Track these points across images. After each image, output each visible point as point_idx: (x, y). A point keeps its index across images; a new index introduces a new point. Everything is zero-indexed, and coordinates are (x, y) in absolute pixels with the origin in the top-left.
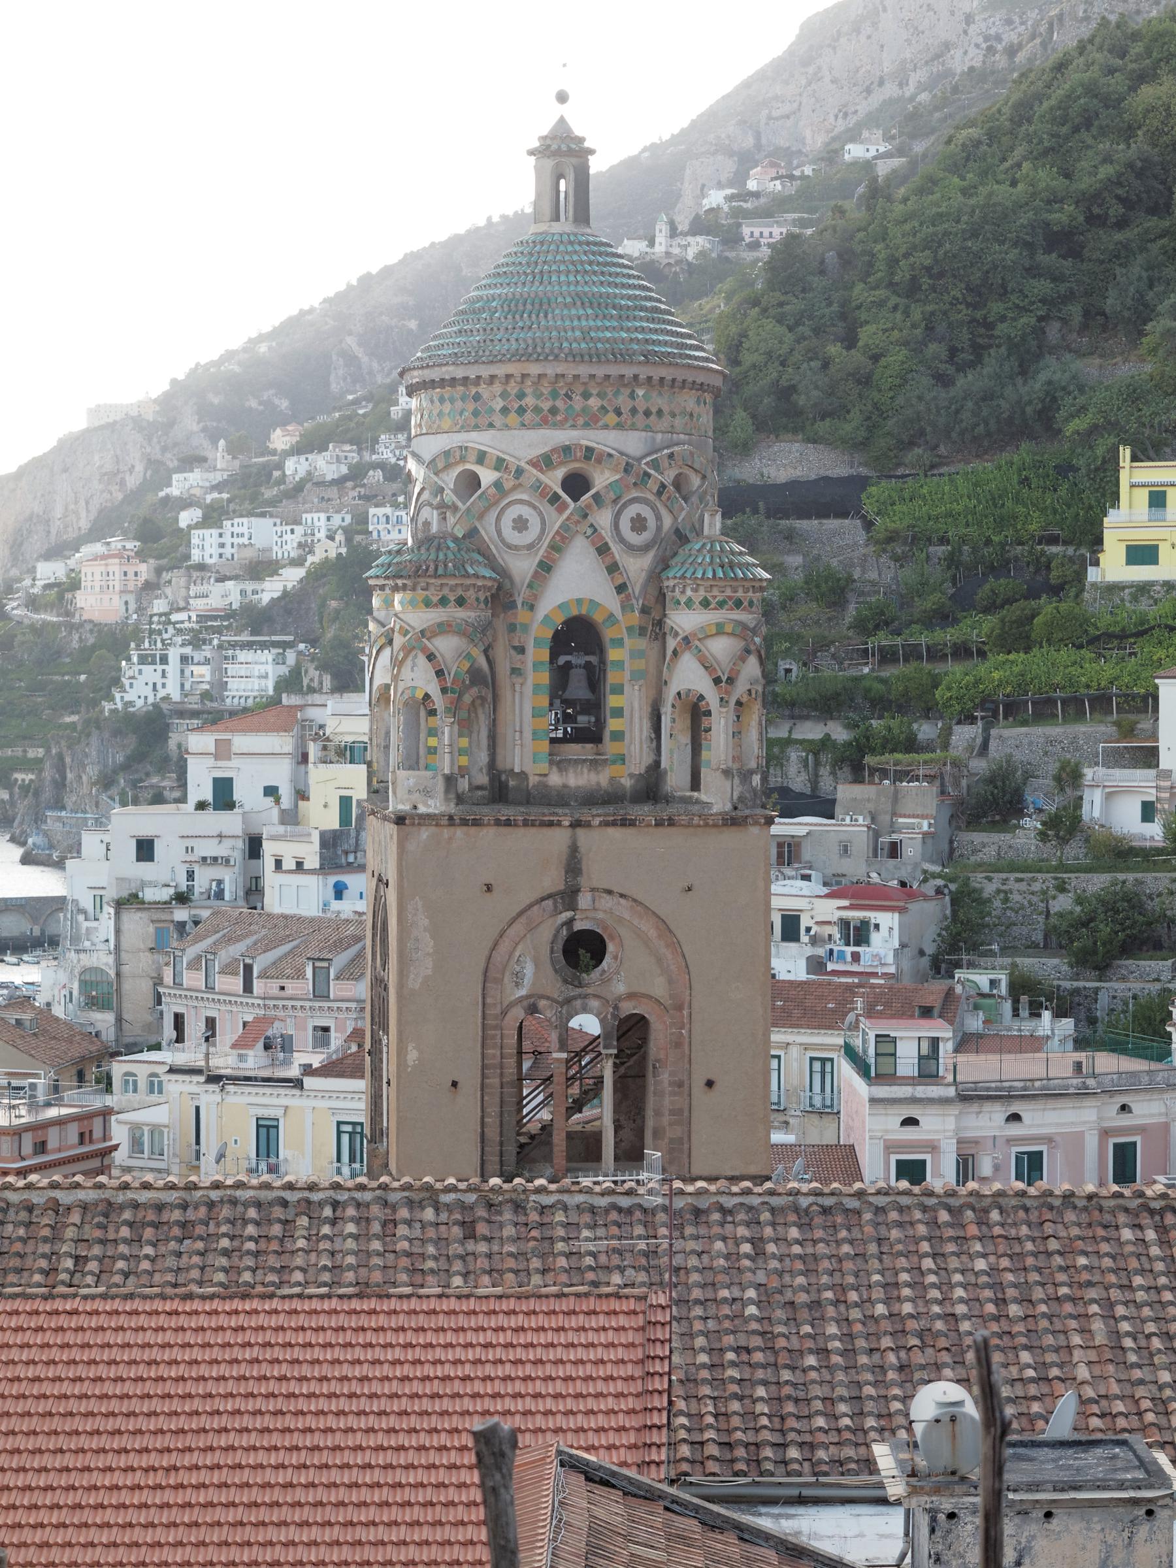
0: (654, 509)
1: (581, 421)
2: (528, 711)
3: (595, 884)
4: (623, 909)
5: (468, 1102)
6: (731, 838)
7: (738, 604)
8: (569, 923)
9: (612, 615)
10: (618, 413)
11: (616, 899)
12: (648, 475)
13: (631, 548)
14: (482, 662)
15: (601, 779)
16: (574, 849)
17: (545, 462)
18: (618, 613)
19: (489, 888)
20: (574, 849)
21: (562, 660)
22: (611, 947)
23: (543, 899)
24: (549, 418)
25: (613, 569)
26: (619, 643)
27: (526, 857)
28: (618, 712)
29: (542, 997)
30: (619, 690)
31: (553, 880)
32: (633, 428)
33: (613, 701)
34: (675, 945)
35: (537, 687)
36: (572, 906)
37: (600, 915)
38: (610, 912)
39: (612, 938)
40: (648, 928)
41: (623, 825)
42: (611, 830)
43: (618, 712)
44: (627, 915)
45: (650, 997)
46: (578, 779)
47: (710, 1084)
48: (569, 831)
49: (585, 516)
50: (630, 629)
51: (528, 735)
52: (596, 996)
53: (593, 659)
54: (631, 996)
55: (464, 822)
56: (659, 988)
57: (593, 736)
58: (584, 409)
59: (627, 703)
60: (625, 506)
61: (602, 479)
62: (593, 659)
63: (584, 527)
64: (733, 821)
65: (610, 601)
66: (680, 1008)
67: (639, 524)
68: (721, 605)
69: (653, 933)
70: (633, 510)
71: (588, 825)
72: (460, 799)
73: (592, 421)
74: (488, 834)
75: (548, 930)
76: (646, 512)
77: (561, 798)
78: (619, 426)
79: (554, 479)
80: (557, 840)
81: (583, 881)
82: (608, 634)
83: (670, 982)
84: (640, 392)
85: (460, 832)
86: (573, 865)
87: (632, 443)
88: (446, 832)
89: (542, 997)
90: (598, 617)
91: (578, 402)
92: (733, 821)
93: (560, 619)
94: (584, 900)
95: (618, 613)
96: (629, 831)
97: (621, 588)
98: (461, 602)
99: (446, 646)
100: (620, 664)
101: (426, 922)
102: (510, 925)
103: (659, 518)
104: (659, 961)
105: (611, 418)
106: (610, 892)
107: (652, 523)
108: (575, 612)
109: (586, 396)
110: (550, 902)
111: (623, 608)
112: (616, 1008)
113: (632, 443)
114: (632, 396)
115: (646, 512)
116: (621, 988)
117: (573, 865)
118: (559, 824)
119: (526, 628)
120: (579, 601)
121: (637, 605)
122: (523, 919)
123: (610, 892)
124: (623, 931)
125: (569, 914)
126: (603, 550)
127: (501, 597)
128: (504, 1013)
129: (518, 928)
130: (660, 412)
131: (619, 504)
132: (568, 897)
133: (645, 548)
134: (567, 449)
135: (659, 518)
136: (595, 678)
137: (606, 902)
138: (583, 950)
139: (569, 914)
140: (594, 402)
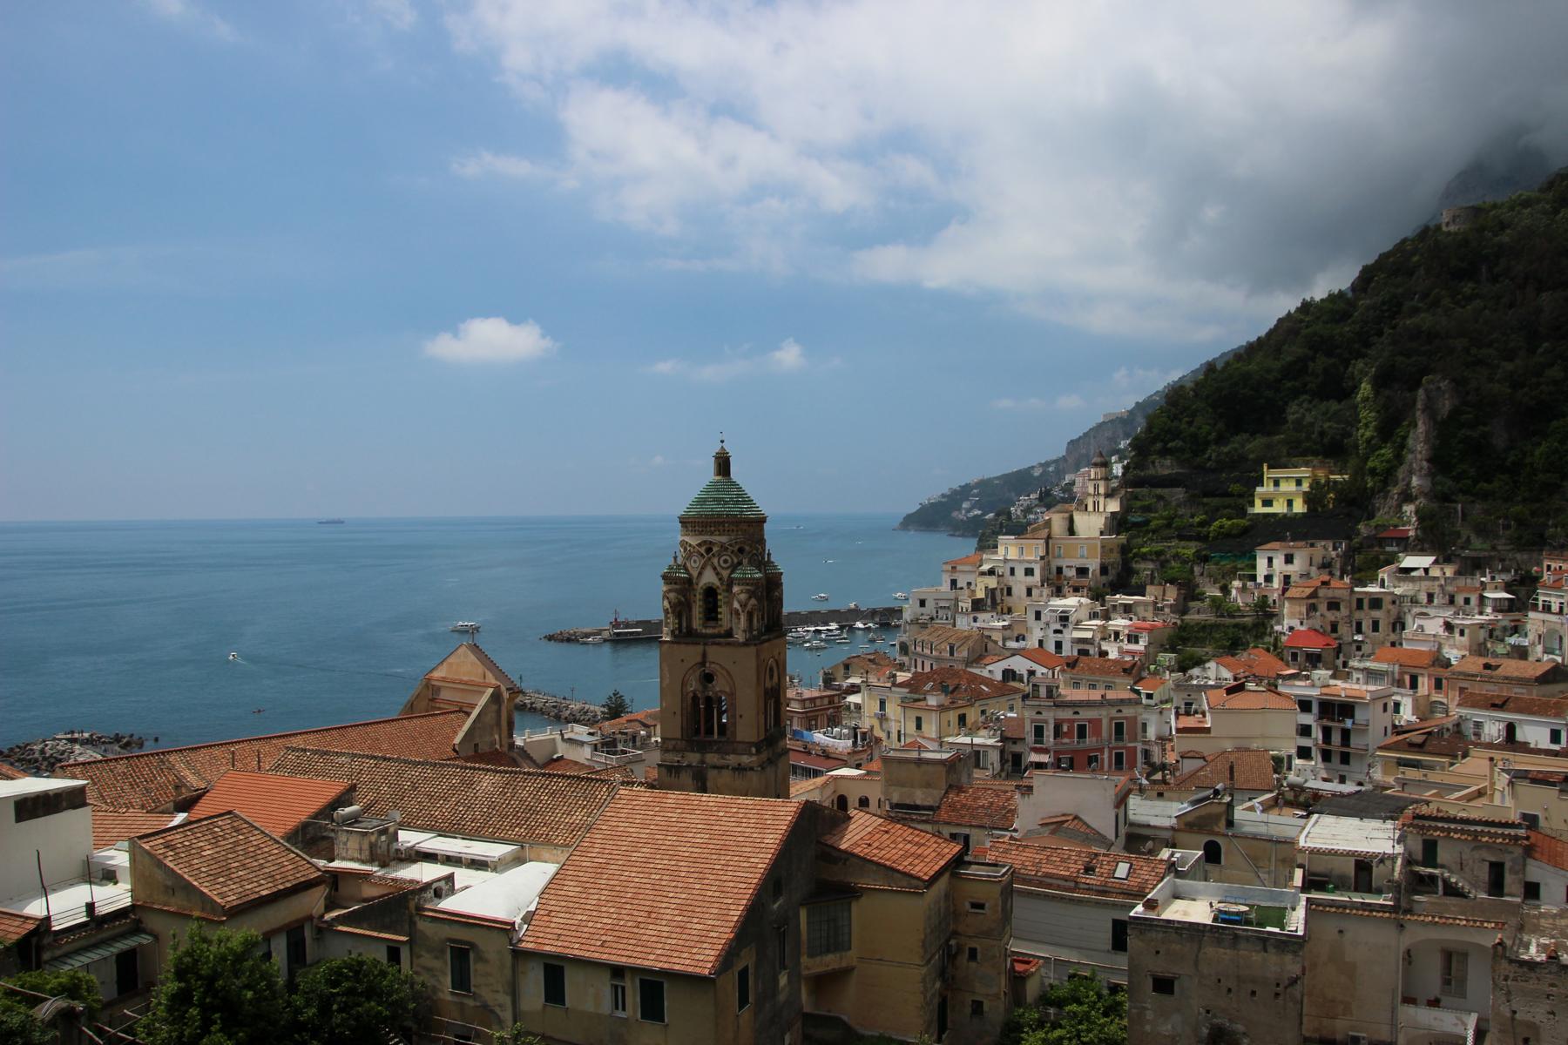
5: (679, 717)
15: (716, 631)
24: (701, 533)
27: (692, 653)
31: (699, 659)
46: (709, 631)
57: (716, 619)
59: (723, 610)
61: (715, 549)
64: (746, 644)
65: (717, 583)
73: (712, 534)
74: (683, 647)
77: (705, 636)
79: (702, 550)
80: (700, 648)
86: (704, 655)
87: (724, 539)
92: (746, 644)
99: (672, 595)
113: (724, 539)
117: (704, 655)
127: (689, 581)
132: (703, 664)
138: (708, 678)
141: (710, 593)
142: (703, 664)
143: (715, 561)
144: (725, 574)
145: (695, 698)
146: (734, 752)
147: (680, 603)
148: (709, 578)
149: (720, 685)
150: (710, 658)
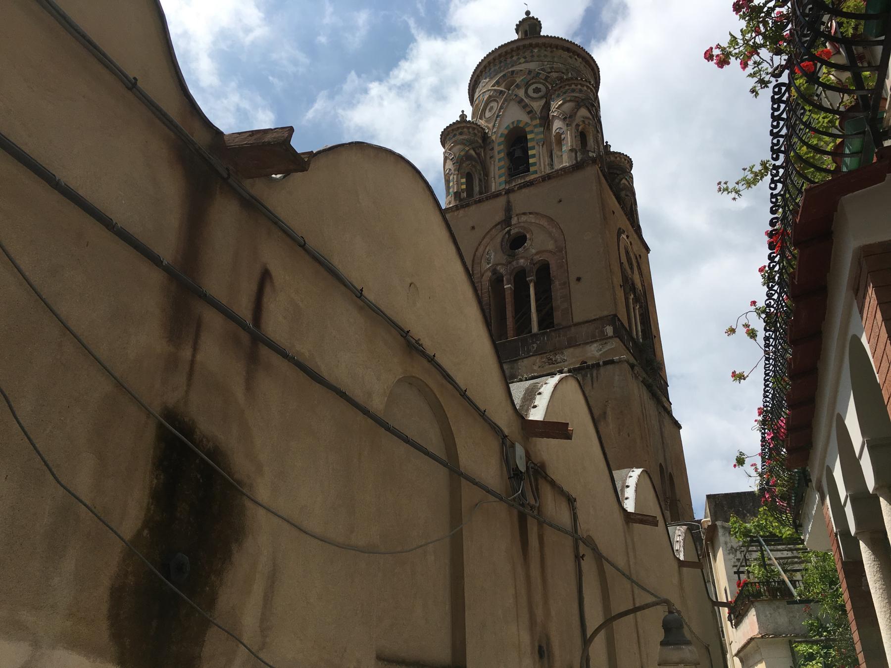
0: (544, 84)
2: (497, 168)
3: (518, 212)
4: (532, 219)
7: (573, 91)
8: (509, 232)
10: (525, 58)
13: (533, 99)
14: (472, 152)
16: (508, 202)
17: (498, 83)
18: (529, 121)
19: (473, 228)
20: (508, 202)
22: (528, 236)
23: (496, 225)
25: (525, 106)
26: (532, 132)
28: (534, 156)
29: (497, 265)
30: (533, 148)
31: (500, 216)
33: (530, 152)
36: (509, 225)
37: (522, 224)
40: (544, 222)
42: (523, 190)
43: (534, 156)
47: (579, 279)
50: (535, 126)
52: (522, 258)
54: (537, 254)
55: (463, 207)
56: (551, 246)
60: (530, 85)
65: (524, 118)
67: (537, 90)
68: (565, 93)
70: (534, 86)
72: (461, 200)
76: (539, 86)
78: (526, 62)
82: (527, 129)
83: (556, 241)
85: (461, 212)
86: (508, 209)
87: (532, 66)
88: (456, 214)
89: (497, 265)
90: (521, 125)
91: (509, 61)
93: (506, 132)
94: (514, 221)
95: (529, 121)
97: (529, 113)
98: (461, 134)
100: (532, 139)
102: (484, 238)
103: (547, 88)
105: (522, 60)
106: (524, 214)
107: (543, 89)
109: (512, 57)
111: (532, 119)
113: (532, 66)
114: (532, 52)
115: (539, 86)
116: (534, 251)
117: (508, 209)
120: (513, 123)
122: (488, 236)
123: (524, 214)
128: (482, 275)
130: (545, 56)
131: (527, 85)
132: (507, 221)
133: (541, 98)
135: (547, 88)
136: (525, 150)
137: (523, 218)
138: (517, 242)
140: (515, 58)
141: (517, 140)
142: (507, 221)
143: (521, 93)
144: (537, 106)
145: (497, 280)
146: (573, 343)
147: (468, 157)
148: (515, 115)
149: (538, 245)
150: (517, 208)
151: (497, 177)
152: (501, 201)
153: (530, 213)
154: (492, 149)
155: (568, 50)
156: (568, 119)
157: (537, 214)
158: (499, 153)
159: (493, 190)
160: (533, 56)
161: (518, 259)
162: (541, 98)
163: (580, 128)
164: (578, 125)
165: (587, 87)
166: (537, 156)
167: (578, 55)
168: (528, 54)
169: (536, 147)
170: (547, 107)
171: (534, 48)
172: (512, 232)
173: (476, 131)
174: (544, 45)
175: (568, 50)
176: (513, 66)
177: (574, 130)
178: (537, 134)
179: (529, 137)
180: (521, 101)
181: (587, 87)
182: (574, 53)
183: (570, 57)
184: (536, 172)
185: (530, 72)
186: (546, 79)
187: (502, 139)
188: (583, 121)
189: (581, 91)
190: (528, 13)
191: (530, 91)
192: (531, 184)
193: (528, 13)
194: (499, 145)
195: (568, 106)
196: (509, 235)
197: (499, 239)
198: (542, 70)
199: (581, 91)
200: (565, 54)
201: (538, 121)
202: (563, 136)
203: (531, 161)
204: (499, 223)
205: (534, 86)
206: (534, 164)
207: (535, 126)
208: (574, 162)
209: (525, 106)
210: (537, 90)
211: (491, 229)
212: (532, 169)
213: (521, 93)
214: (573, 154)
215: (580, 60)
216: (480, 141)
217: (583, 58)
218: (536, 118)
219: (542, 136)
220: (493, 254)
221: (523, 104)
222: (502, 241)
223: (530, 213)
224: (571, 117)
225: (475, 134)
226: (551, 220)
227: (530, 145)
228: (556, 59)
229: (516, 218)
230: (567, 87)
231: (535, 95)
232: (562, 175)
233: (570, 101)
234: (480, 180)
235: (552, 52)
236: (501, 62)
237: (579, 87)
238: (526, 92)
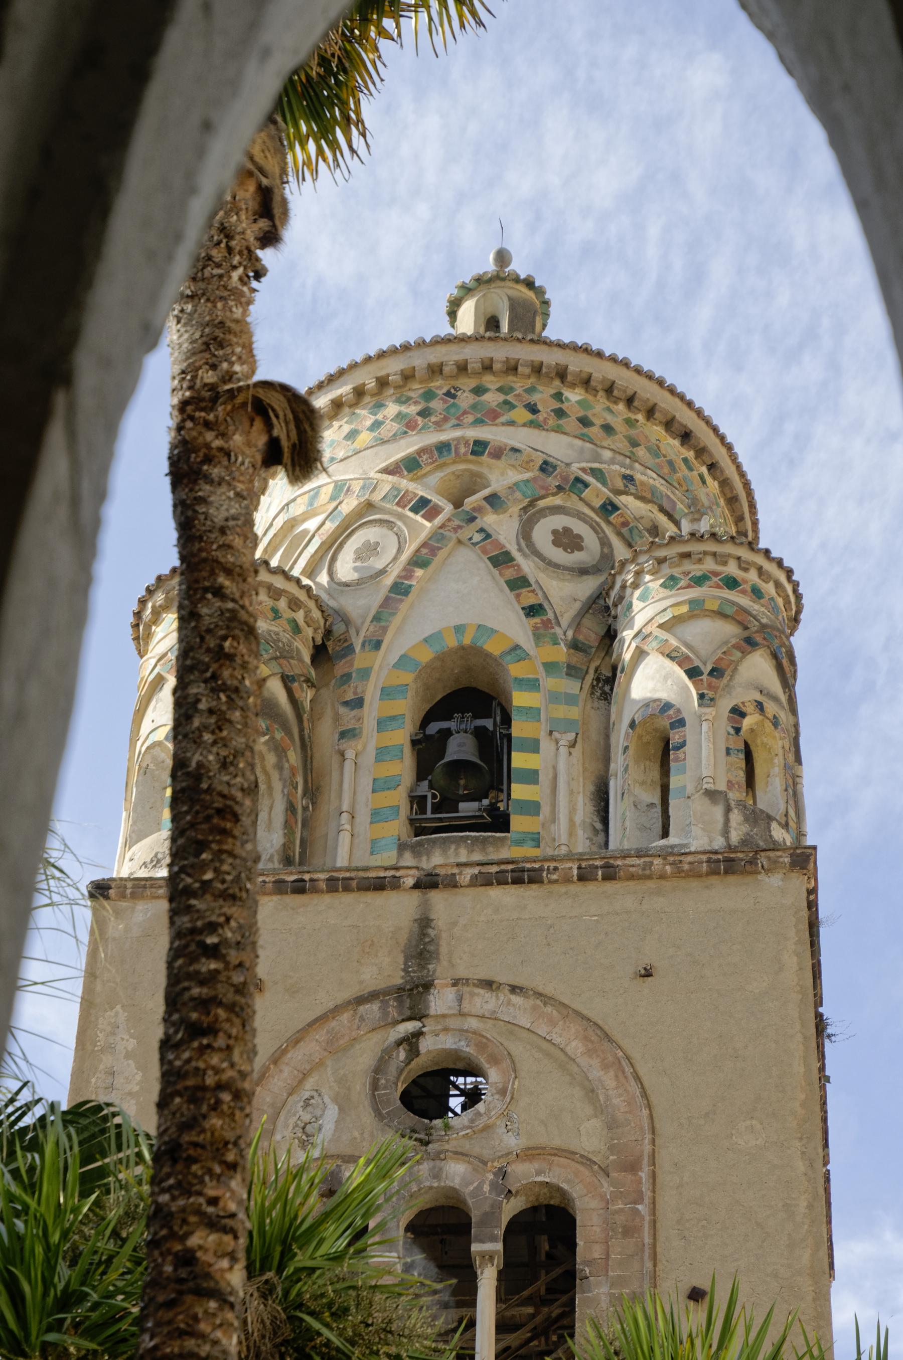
0: (595, 528)
1: (470, 418)
2: (366, 783)
3: (462, 972)
4: (519, 1010)
6: (728, 895)
7: (732, 583)
8: (411, 1041)
9: (517, 647)
11: (504, 995)
12: (586, 485)
16: (424, 923)
17: (410, 466)
20: (424, 923)
21: (434, 728)
23: (360, 1000)
25: (519, 583)
26: (533, 685)
28: (531, 777)
30: (533, 746)
31: (385, 969)
32: (558, 430)
33: (519, 760)
34: (624, 1065)
35: (382, 754)
37: (473, 1023)
38: (494, 1018)
39: (494, 1060)
41: (518, 881)
42: (496, 893)
43: (531, 777)
44: (525, 1022)
45: (570, 1154)
48: (417, 894)
49: (472, 519)
50: (550, 667)
51: (363, 817)
52: (460, 1155)
53: (488, 723)
54: (530, 1153)
56: (590, 1138)
58: (474, 407)
62: (488, 723)
63: (470, 532)
66: (633, 1167)
67: (566, 540)
69: (576, 1047)
70: (559, 522)
71: (452, 884)
75: (370, 1044)
76: (579, 528)
81: (441, 971)
82: (516, 670)
83: (612, 1125)
84: (574, 396)
86: (422, 948)
87: (559, 446)
90: (493, 648)
91: (465, 399)
93: (426, 656)
94: (441, 1001)
96: (528, 893)
97: (532, 611)
100: (532, 713)
101: (132, 1044)
103: (604, 542)
104: (591, 1093)
105: (521, 414)
106: (488, 984)
108: (452, 642)
109: (479, 391)
110: (373, 1009)
111: (537, 638)
112: (502, 1173)
113: (559, 446)
116: (512, 1142)
117: (422, 948)
118: (395, 884)
119: (365, 673)
120: (459, 629)
121: (564, 631)
122: (321, 1035)
123: (488, 984)
124: (517, 1049)
125: (411, 1026)
126: (501, 560)
129: (311, 1048)
130: (608, 429)
132: (412, 996)
133: (583, 571)
134: (443, 447)
135: (604, 542)
139: (411, 1026)
140: (492, 398)
143: (504, 527)
144: (565, 595)
151: (363, 817)
152: (398, 909)
153: (514, 989)
154: (359, 703)
155: (686, 437)
156: (708, 675)
157: (539, 995)
158: (382, 724)
159: (342, 861)
160: (560, 413)
161: (438, 1156)
162: (583, 571)
163: (747, 723)
164: (738, 713)
165: (778, 585)
166: (544, 778)
167: (712, 467)
168: (543, 396)
169: (546, 745)
170: (603, 617)
171: (573, 386)
172: (426, 1045)
173: (300, 616)
174: (609, 389)
175: (686, 437)
176: (479, 422)
177: (725, 726)
178: (554, 698)
179: (520, 699)
180: (501, 560)
181: (778, 585)
182: (701, 452)
183: (685, 460)
184: (536, 840)
185: (546, 467)
186: (609, 508)
187: (407, 678)
188: (760, 706)
189: (757, 593)
190: (502, 257)
191: (542, 533)
192: (521, 876)
193: (502, 257)
194: (387, 693)
195: (709, 635)
196: (414, 1052)
197: (364, 1056)
198: (597, 473)
199: (757, 593)
200: (672, 445)
201: (561, 654)
202: (675, 738)
203: (519, 791)
204: (373, 996)
205: (559, 522)
206: (532, 808)
207: (550, 667)
208: (719, 843)
209: (519, 583)
210: (566, 540)
211: (336, 1010)
212: (518, 823)
213: (504, 527)
214: (718, 812)
215: (713, 485)
216: (307, 659)
217: (725, 483)
218: (556, 643)
219: (574, 713)
220: (332, 1112)
221: (510, 573)
222: (379, 1069)
223: (514, 989)
224: (716, 672)
225: (296, 629)
226: (599, 1035)
227: (519, 729)
228: (641, 452)
229: (450, 994)
230: (709, 565)
231: (558, 555)
232: (662, 877)
233: (721, 614)
234: (291, 808)
235: (630, 423)
236: (429, 395)
237: (752, 576)
238: (525, 533)
